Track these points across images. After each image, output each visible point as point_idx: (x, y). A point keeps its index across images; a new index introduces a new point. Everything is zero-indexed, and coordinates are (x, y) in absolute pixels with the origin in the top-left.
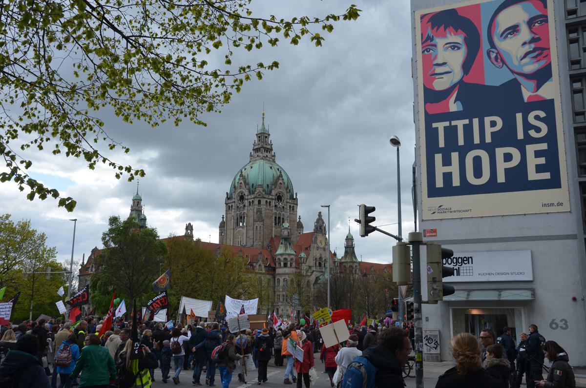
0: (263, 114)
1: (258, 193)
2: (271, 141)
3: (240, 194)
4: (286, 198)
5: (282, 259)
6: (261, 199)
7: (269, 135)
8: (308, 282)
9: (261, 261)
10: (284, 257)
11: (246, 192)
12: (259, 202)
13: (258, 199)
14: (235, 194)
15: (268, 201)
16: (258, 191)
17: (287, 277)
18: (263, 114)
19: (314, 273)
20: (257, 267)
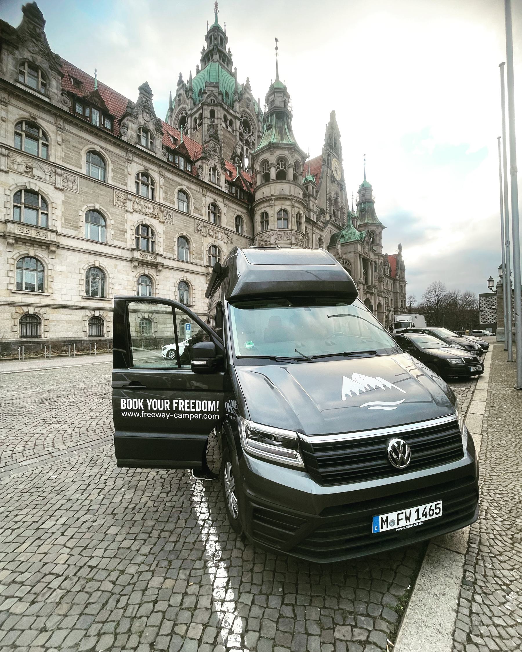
0: (216, 5)
1: (209, 96)
2: (229, 49)
3: (180, 116)
4: (257, 130)
5: (272, 159)
6: (215, 109)
7: (226, 39)
8: (320, 239)
9: (216, 159)
10: (278, 153)
11: (188, 105)
12: (212, 114)
13: (210, 108)
14: (171, 120)
15: (229, 117)
16: (208, 93)
17: (287, 205)
18: (216, 5)
19: (329, 225)
20: (206, 168)
